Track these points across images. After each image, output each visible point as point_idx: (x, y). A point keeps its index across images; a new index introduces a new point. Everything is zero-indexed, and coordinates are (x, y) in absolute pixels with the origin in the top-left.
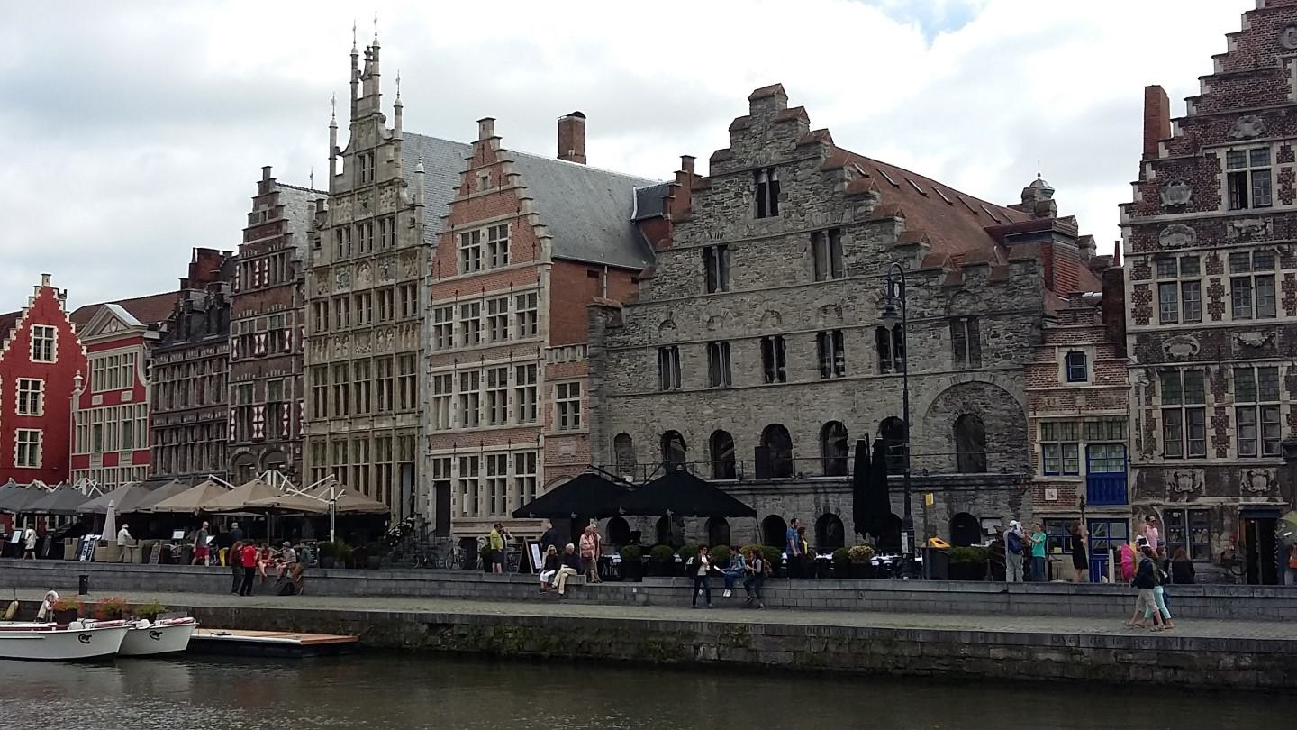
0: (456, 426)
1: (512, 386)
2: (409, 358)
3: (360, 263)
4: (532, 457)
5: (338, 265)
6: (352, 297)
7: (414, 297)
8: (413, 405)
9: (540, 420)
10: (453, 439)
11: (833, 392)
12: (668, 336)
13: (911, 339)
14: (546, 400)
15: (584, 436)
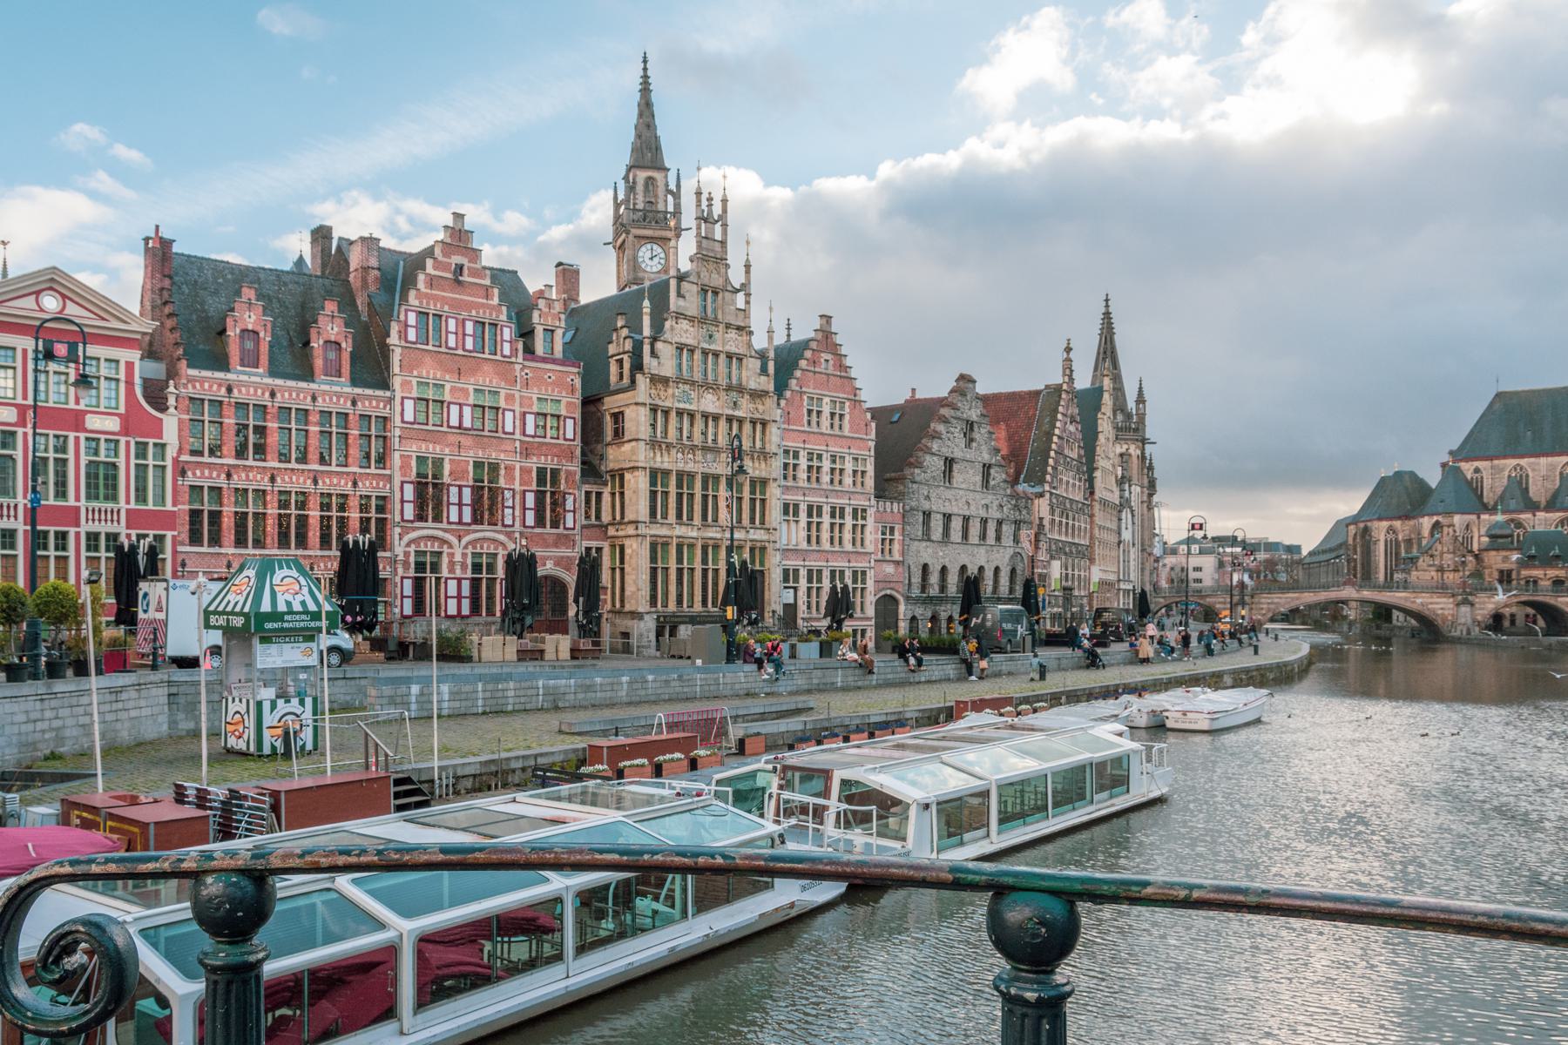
0: (804, 545)
1: (849, 521)
2: (761, 484)
3: (707, 386)
4: (864, 573)
5: (680, 380)
6: (698, 417)
7: (763, 432)
8: (762, 523)
9: (870, 547)
10: (803, 554)
11: (982, 550)
12: (926, 506)
13: (1004, 527)
14: (872, 536)
15: (897, 563)
